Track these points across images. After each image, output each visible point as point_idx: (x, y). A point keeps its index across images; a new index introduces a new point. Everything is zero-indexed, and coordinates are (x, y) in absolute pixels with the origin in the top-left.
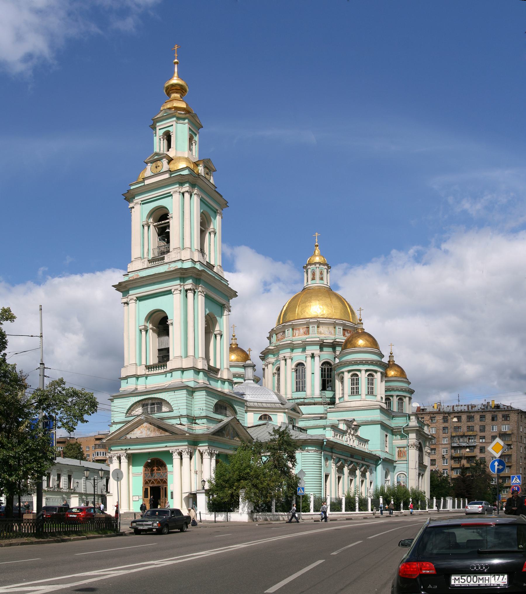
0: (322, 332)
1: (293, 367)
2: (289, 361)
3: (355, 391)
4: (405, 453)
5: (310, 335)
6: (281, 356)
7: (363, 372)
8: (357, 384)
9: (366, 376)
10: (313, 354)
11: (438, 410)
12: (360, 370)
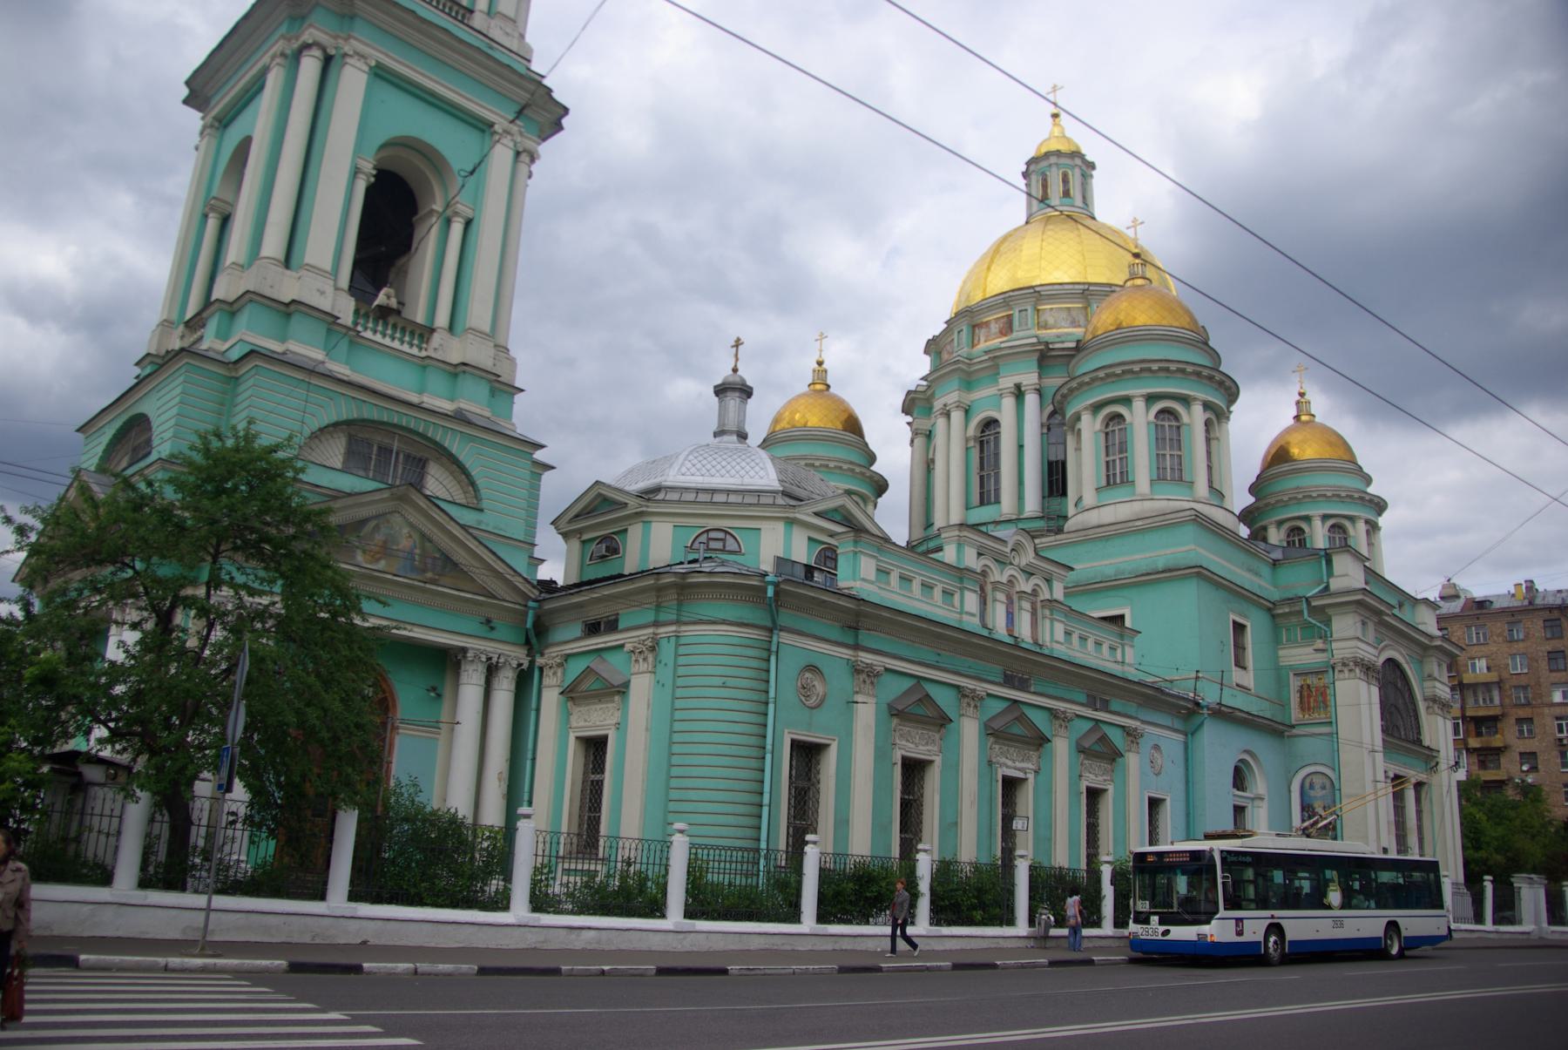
0: (1051, 321)
1: (971, 432)
2: (957, 416)
3: (1116, 477)
4: (1324, 694)
5: (1015, 335)
6: (938, 405)
7: (1139, 405)
8: (1123, 448)
9: (1151, 416)
10: (1018, 386)
11: (1526, 603)
12: (1127, 401)
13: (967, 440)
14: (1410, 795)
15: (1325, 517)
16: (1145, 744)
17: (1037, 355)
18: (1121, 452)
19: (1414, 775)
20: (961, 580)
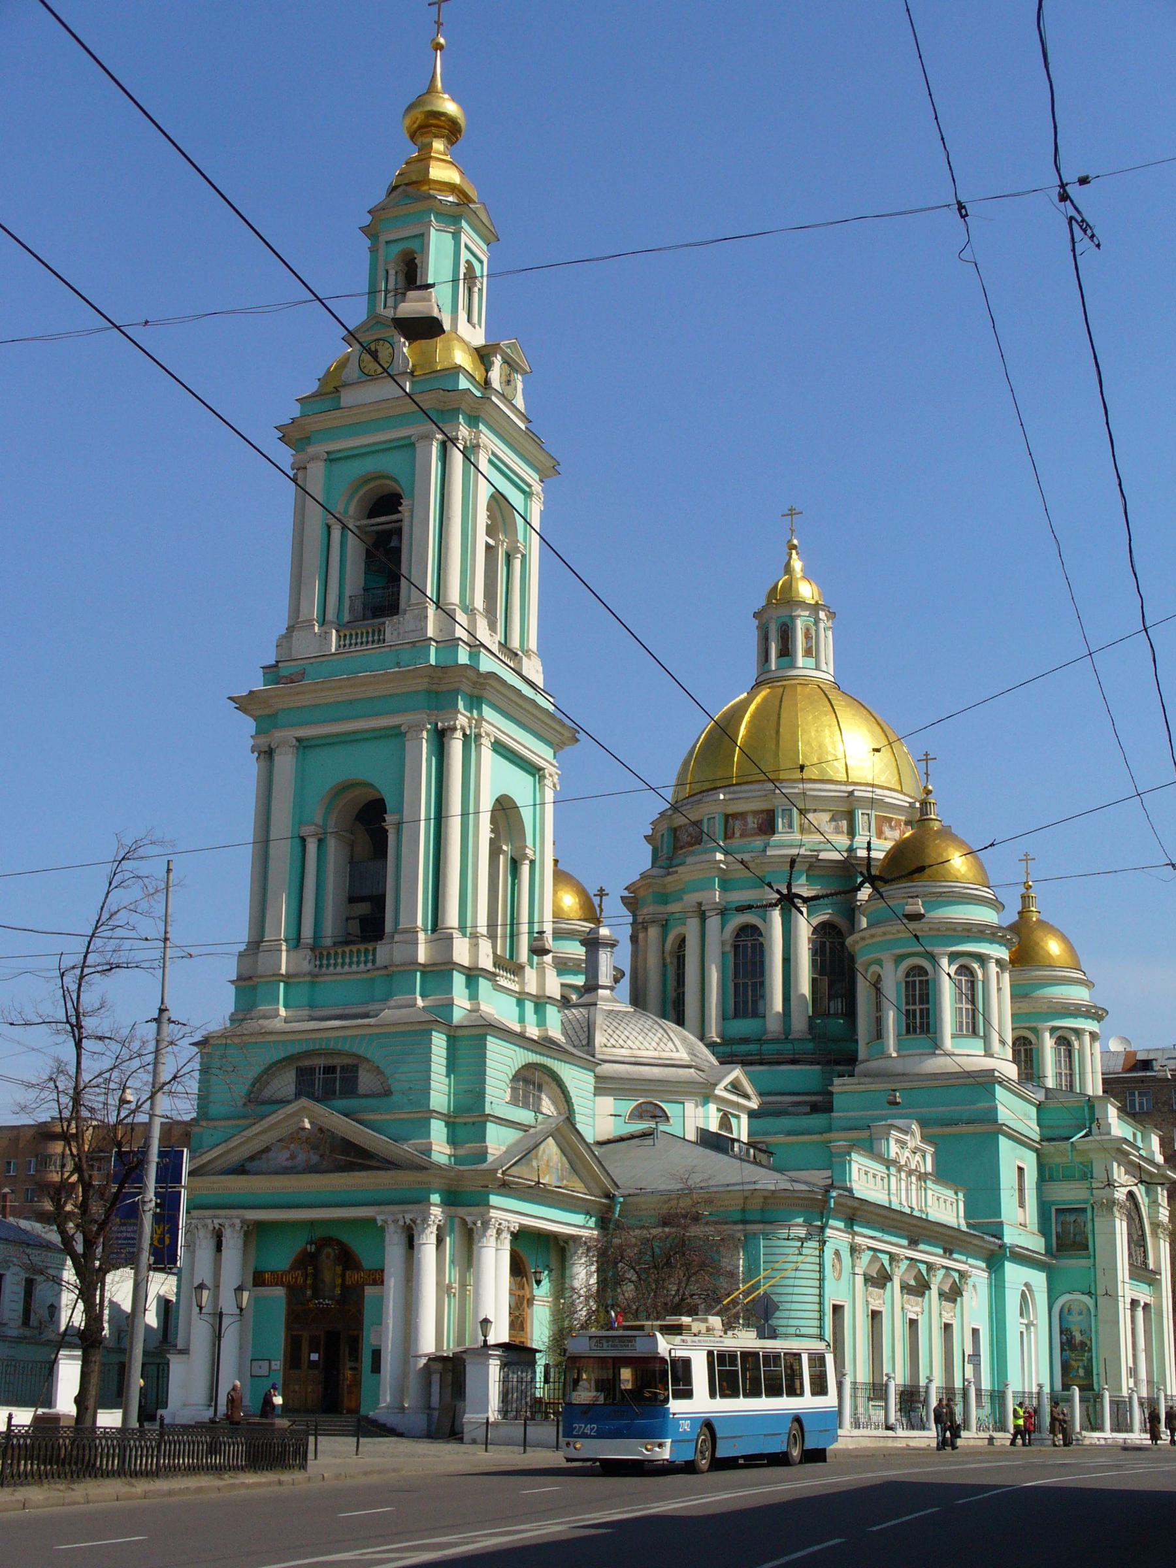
13: (723, 943)
14: (1140, 1313)
15: (1053, 1030)
16: (970, 1281)
17: (807, 865)
18: (921, 1003)
19: (1144, 1299)
20: (888, 1168)
